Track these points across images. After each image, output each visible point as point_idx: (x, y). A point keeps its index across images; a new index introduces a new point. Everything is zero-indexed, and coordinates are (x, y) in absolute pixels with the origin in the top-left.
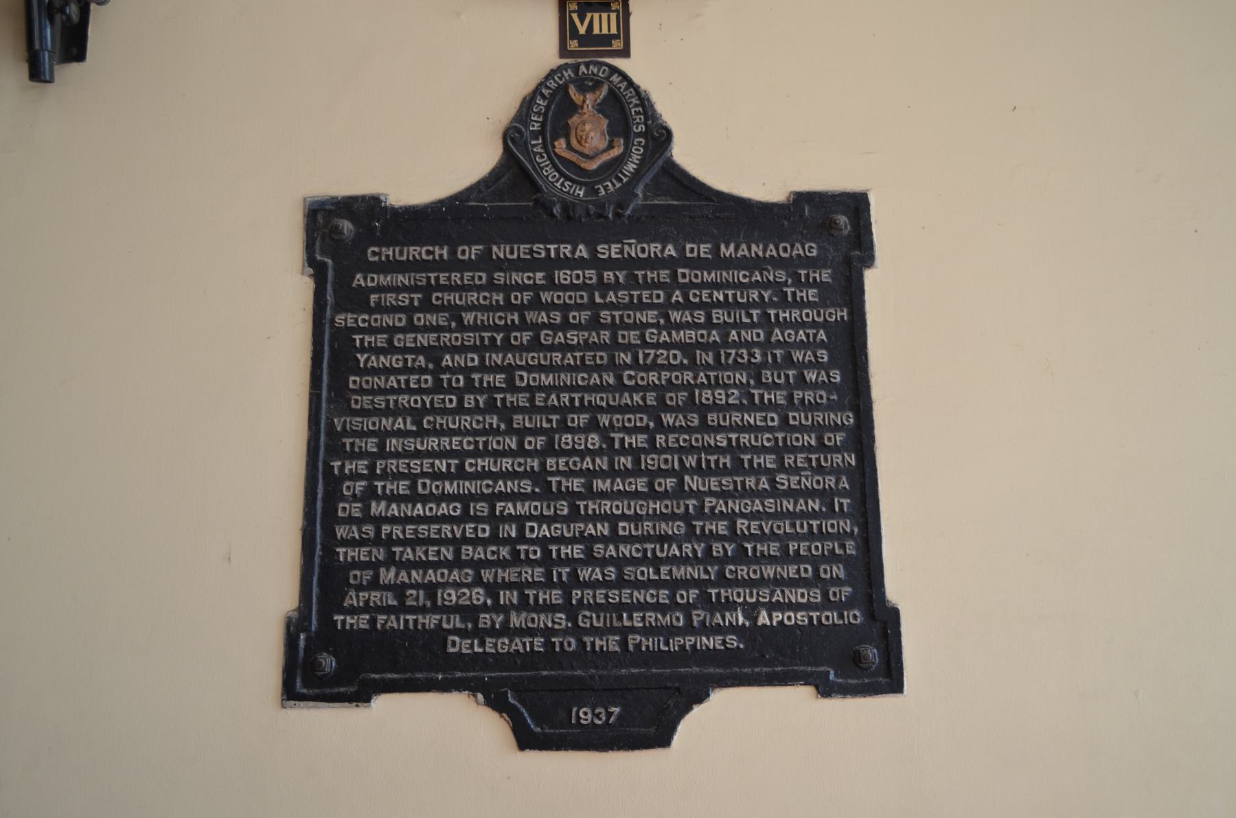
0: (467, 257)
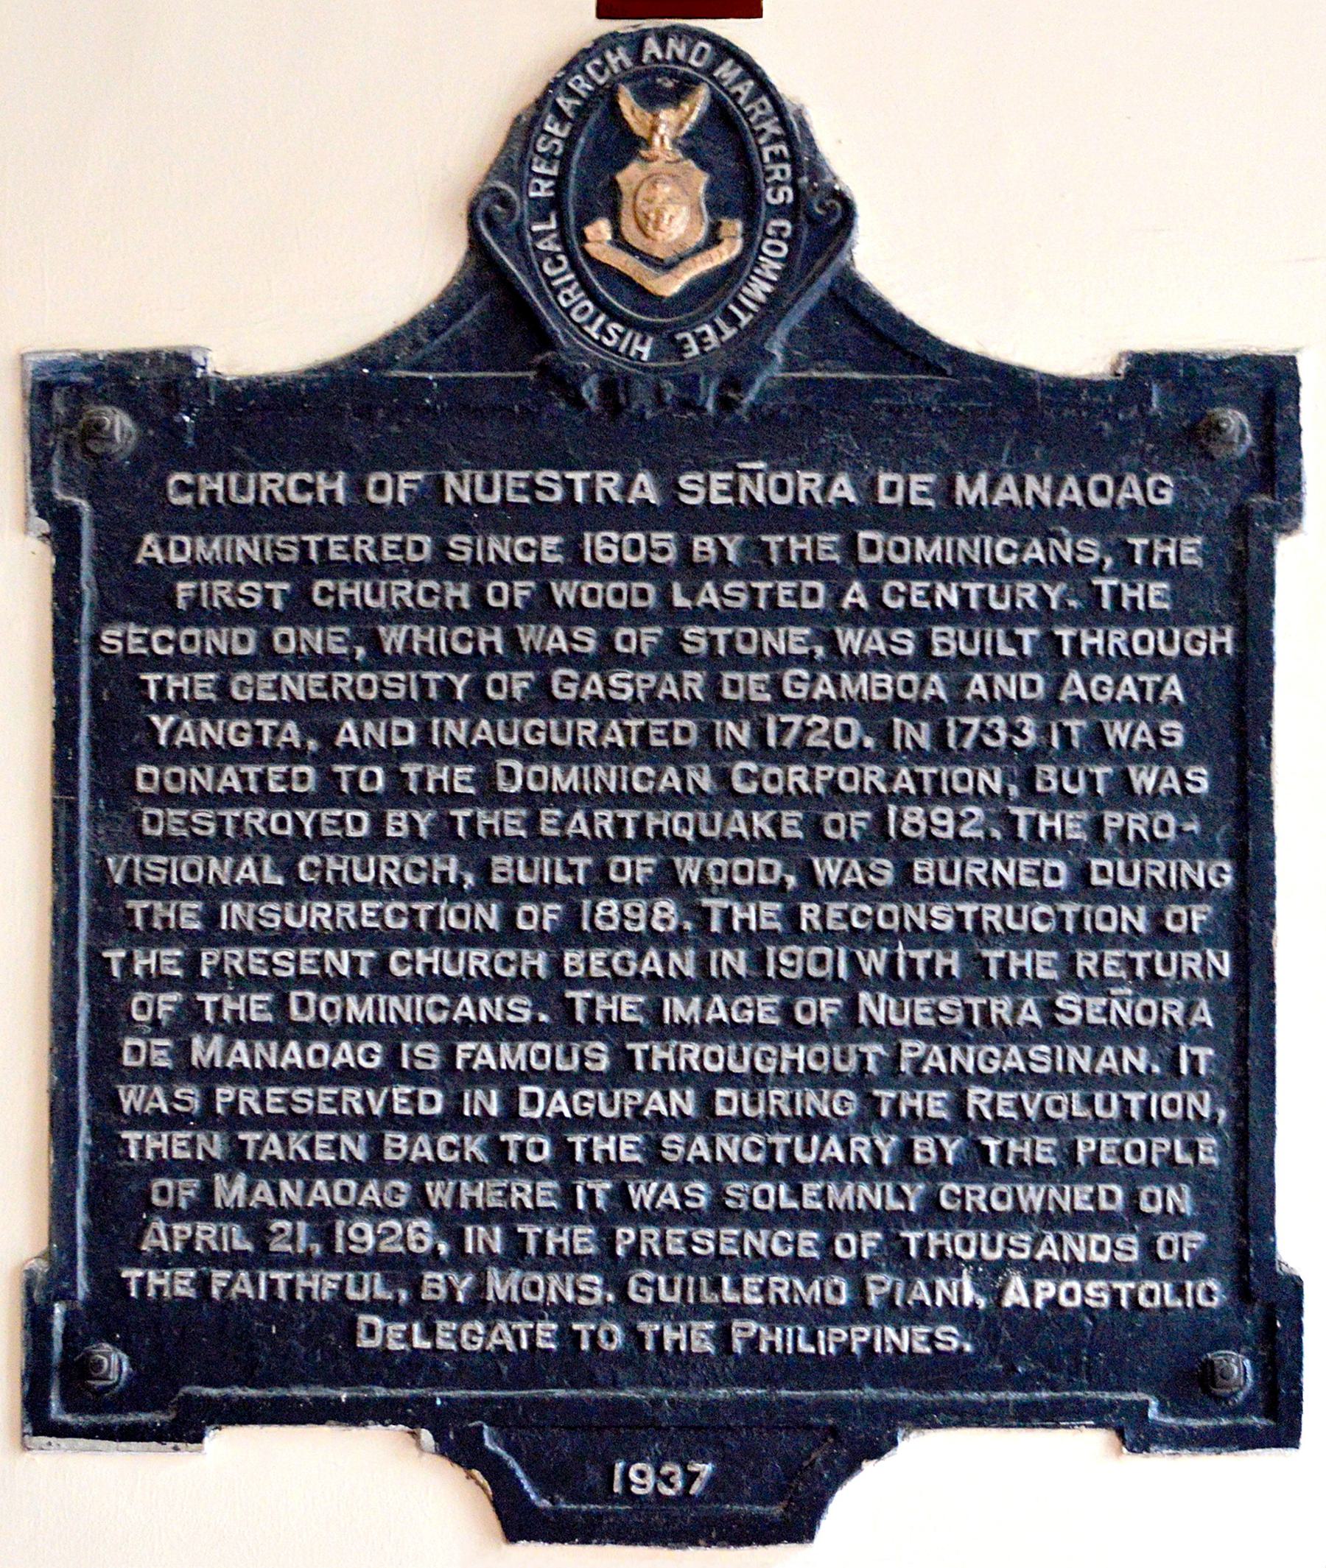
0: (387, 498)
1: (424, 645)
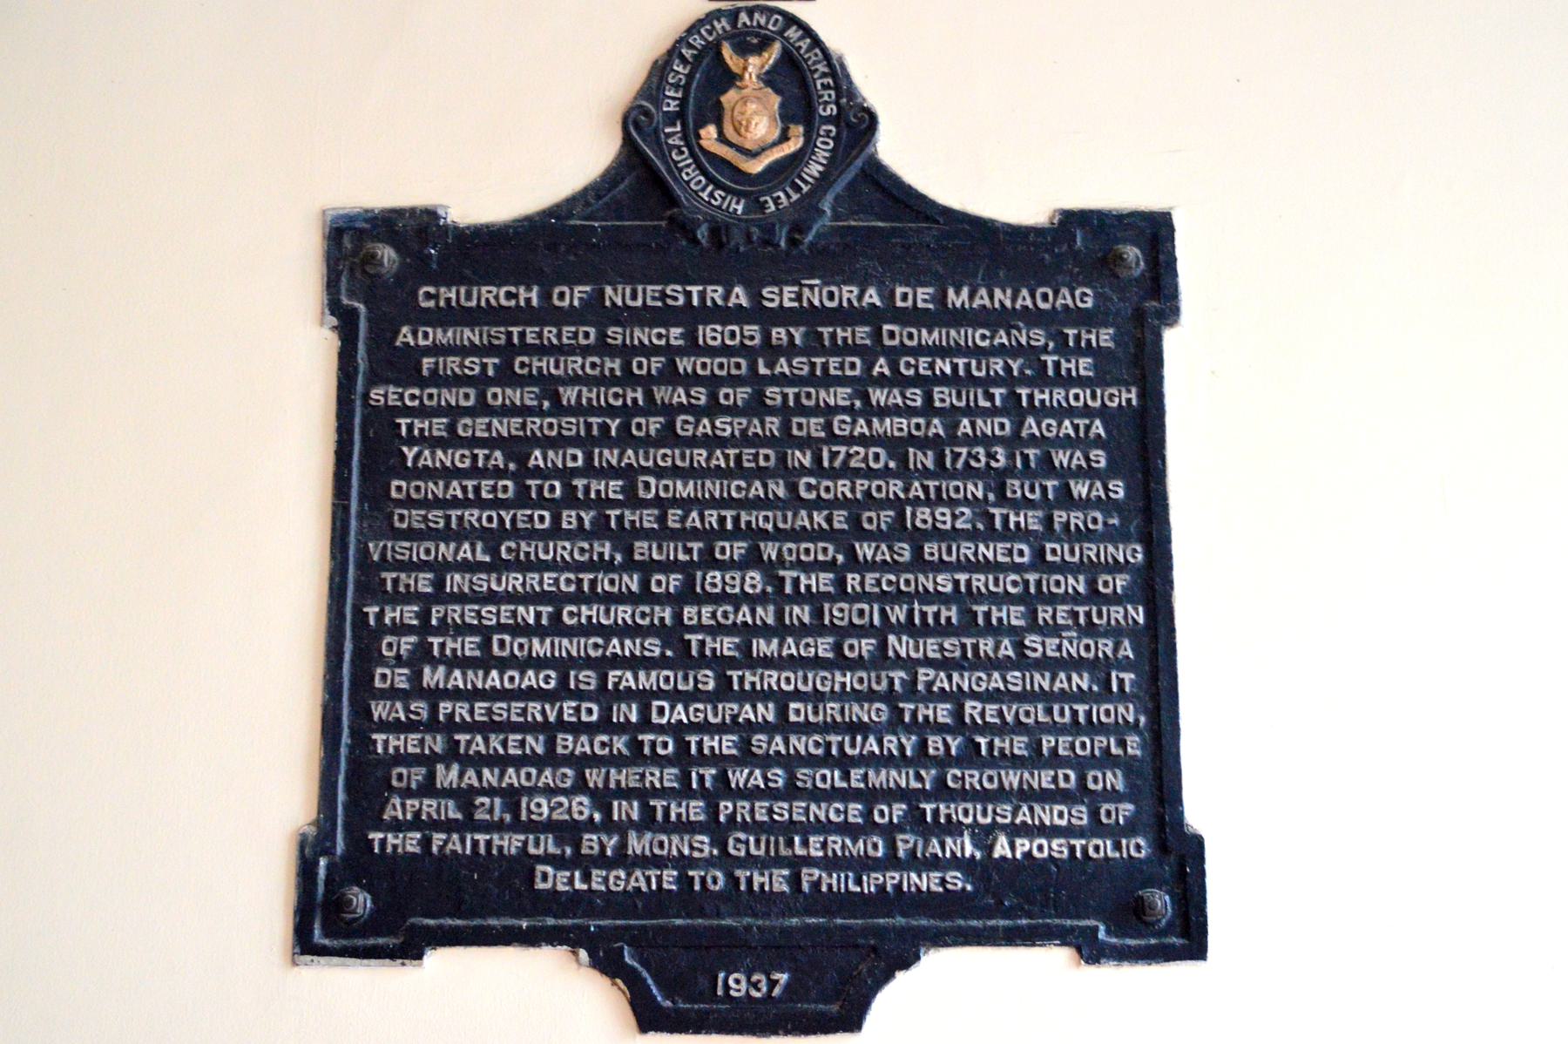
0: (566, 303)
1: (590, 400)
